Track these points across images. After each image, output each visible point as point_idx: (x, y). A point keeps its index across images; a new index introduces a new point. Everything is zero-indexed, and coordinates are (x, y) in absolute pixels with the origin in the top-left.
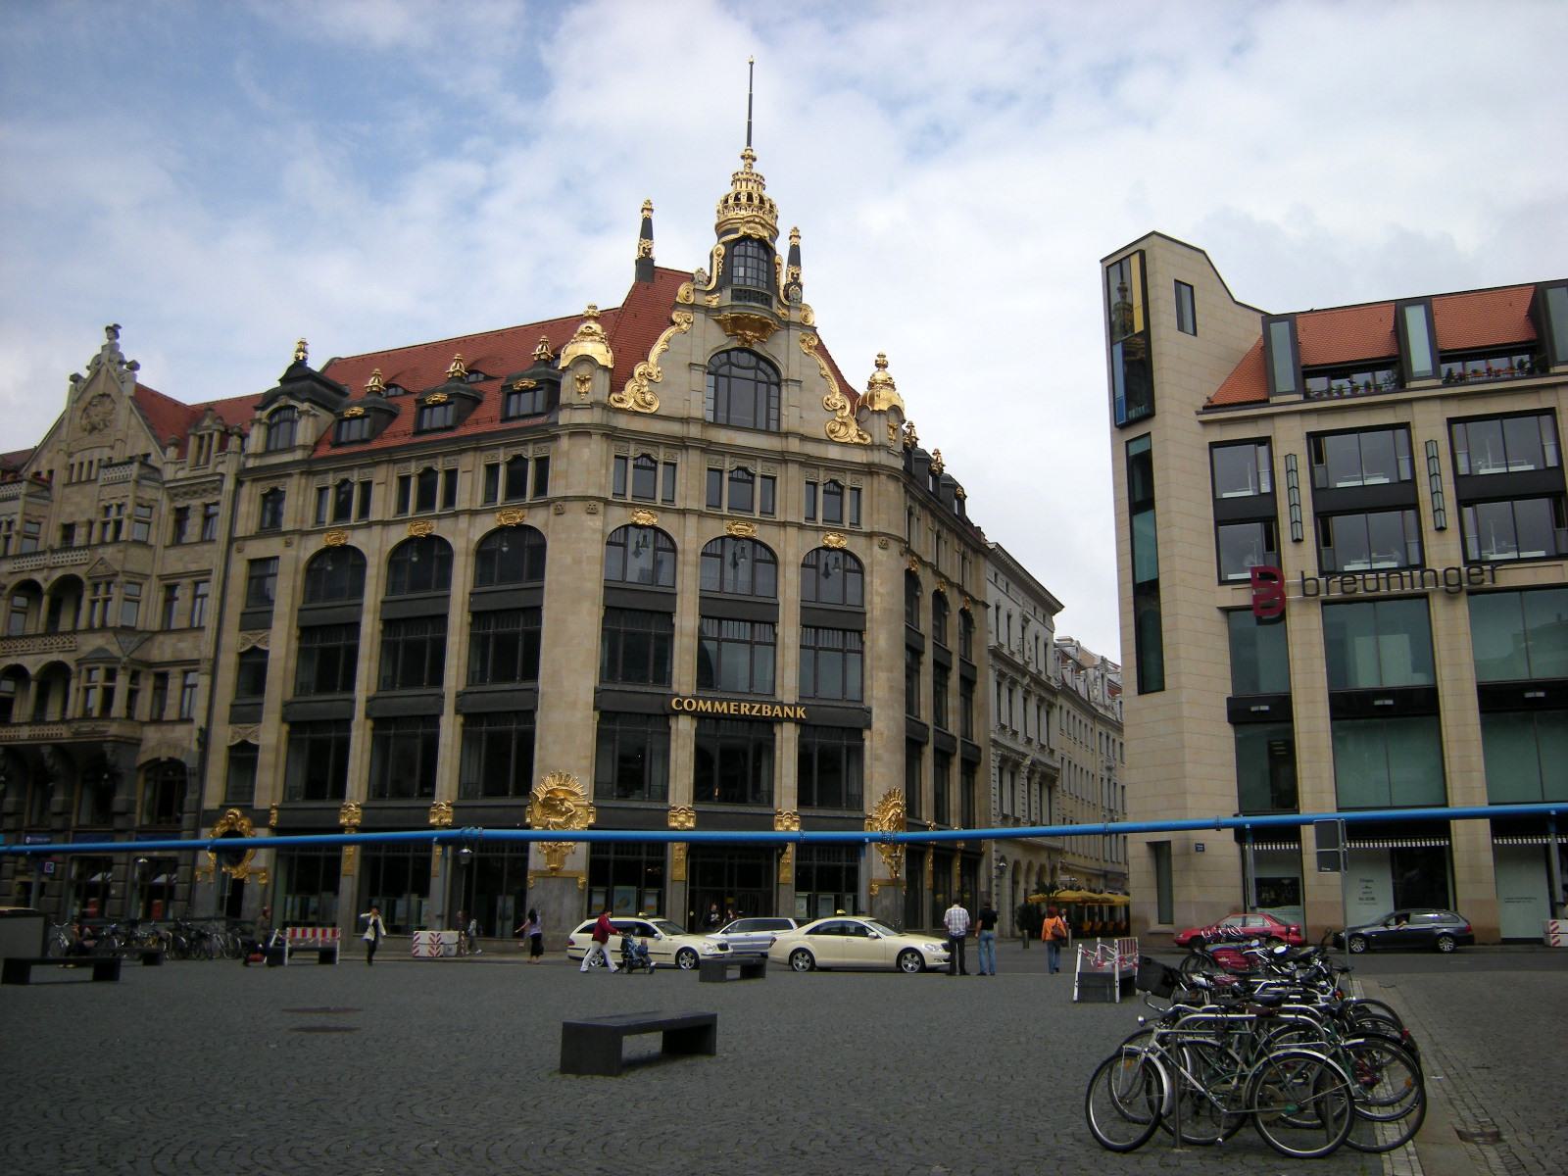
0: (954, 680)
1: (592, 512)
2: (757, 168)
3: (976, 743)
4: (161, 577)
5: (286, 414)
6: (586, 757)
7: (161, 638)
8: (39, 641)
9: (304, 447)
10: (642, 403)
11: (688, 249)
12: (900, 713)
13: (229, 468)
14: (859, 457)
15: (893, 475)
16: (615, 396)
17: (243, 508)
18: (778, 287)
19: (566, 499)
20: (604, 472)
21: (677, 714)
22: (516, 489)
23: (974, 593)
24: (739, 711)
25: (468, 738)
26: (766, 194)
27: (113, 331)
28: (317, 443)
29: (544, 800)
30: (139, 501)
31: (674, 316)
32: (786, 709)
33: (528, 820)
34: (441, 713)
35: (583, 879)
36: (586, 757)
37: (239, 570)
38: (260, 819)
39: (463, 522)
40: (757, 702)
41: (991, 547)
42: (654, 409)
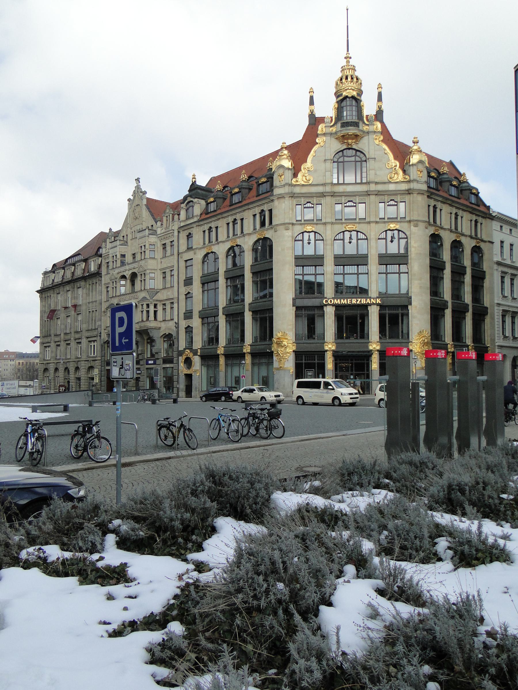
0: (468, 279)
1: (287, 229)
2: (352, 62)
3: (485, 305)
4: (160, 270)
5: (191, 204)
7: (163, 291)
8: (128, 296)
9: (197, 216)
10: (305, 181)
11: (326, 108)
12: (427, 298)
13: (176, 228)
14: (404, 187)
15: (420, 192)
16: (294, 180)
17: (181, 242)
18: (363, 117)
19: (277, 225)
20: (291, 212)
21: (326, 305)
22: (263, 224)
23: (484, 238)
25: (254, 319)
26: (357, 74)
27: (138, 180)
28: (201, 214)
30: (150, 243)
31: (317, 141)
32: (372, 300)
35: (291, 371)
37: (182, 264)
38: (195, 353)
39: (247, 238)
40: (359, 298)
41: (494, 214)
42: (310, 182)
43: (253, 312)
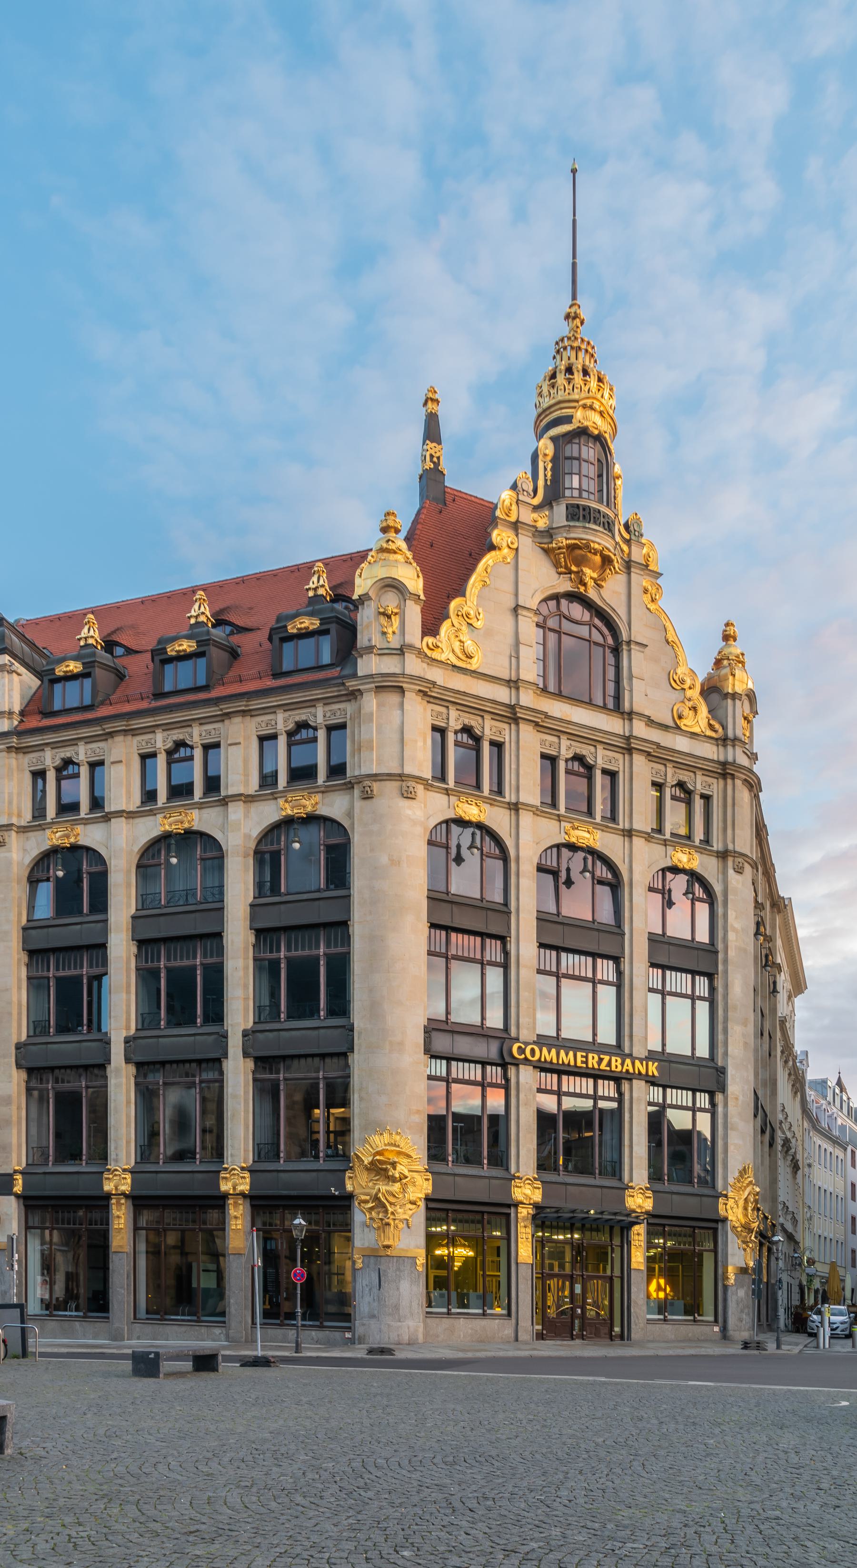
6: (418, 1112)
24: (586, 1062)
29: (372, 1163)
32: (637, 1063)
33: (349, 1187)
34: (226, 1056)
36: (418, 1112)
43: (258, 1060)
